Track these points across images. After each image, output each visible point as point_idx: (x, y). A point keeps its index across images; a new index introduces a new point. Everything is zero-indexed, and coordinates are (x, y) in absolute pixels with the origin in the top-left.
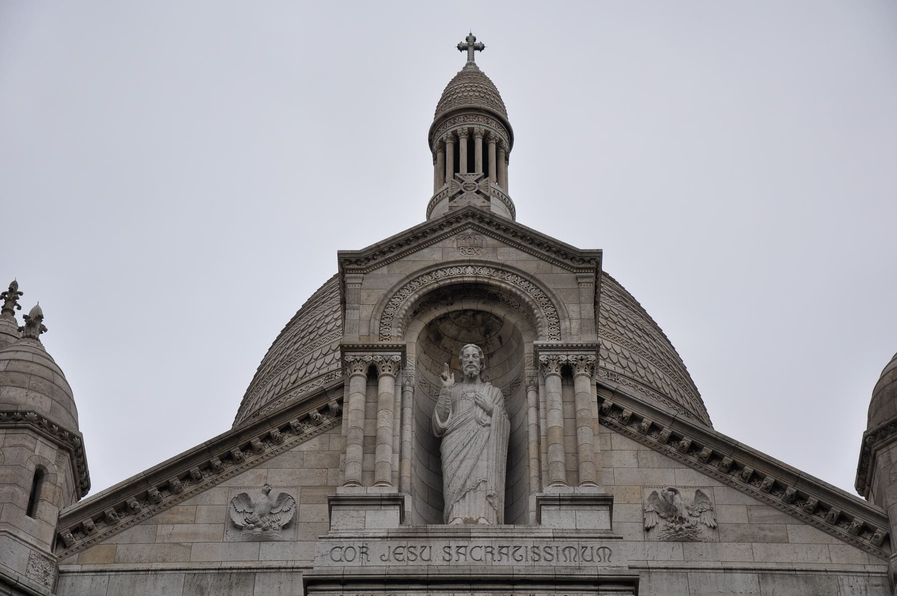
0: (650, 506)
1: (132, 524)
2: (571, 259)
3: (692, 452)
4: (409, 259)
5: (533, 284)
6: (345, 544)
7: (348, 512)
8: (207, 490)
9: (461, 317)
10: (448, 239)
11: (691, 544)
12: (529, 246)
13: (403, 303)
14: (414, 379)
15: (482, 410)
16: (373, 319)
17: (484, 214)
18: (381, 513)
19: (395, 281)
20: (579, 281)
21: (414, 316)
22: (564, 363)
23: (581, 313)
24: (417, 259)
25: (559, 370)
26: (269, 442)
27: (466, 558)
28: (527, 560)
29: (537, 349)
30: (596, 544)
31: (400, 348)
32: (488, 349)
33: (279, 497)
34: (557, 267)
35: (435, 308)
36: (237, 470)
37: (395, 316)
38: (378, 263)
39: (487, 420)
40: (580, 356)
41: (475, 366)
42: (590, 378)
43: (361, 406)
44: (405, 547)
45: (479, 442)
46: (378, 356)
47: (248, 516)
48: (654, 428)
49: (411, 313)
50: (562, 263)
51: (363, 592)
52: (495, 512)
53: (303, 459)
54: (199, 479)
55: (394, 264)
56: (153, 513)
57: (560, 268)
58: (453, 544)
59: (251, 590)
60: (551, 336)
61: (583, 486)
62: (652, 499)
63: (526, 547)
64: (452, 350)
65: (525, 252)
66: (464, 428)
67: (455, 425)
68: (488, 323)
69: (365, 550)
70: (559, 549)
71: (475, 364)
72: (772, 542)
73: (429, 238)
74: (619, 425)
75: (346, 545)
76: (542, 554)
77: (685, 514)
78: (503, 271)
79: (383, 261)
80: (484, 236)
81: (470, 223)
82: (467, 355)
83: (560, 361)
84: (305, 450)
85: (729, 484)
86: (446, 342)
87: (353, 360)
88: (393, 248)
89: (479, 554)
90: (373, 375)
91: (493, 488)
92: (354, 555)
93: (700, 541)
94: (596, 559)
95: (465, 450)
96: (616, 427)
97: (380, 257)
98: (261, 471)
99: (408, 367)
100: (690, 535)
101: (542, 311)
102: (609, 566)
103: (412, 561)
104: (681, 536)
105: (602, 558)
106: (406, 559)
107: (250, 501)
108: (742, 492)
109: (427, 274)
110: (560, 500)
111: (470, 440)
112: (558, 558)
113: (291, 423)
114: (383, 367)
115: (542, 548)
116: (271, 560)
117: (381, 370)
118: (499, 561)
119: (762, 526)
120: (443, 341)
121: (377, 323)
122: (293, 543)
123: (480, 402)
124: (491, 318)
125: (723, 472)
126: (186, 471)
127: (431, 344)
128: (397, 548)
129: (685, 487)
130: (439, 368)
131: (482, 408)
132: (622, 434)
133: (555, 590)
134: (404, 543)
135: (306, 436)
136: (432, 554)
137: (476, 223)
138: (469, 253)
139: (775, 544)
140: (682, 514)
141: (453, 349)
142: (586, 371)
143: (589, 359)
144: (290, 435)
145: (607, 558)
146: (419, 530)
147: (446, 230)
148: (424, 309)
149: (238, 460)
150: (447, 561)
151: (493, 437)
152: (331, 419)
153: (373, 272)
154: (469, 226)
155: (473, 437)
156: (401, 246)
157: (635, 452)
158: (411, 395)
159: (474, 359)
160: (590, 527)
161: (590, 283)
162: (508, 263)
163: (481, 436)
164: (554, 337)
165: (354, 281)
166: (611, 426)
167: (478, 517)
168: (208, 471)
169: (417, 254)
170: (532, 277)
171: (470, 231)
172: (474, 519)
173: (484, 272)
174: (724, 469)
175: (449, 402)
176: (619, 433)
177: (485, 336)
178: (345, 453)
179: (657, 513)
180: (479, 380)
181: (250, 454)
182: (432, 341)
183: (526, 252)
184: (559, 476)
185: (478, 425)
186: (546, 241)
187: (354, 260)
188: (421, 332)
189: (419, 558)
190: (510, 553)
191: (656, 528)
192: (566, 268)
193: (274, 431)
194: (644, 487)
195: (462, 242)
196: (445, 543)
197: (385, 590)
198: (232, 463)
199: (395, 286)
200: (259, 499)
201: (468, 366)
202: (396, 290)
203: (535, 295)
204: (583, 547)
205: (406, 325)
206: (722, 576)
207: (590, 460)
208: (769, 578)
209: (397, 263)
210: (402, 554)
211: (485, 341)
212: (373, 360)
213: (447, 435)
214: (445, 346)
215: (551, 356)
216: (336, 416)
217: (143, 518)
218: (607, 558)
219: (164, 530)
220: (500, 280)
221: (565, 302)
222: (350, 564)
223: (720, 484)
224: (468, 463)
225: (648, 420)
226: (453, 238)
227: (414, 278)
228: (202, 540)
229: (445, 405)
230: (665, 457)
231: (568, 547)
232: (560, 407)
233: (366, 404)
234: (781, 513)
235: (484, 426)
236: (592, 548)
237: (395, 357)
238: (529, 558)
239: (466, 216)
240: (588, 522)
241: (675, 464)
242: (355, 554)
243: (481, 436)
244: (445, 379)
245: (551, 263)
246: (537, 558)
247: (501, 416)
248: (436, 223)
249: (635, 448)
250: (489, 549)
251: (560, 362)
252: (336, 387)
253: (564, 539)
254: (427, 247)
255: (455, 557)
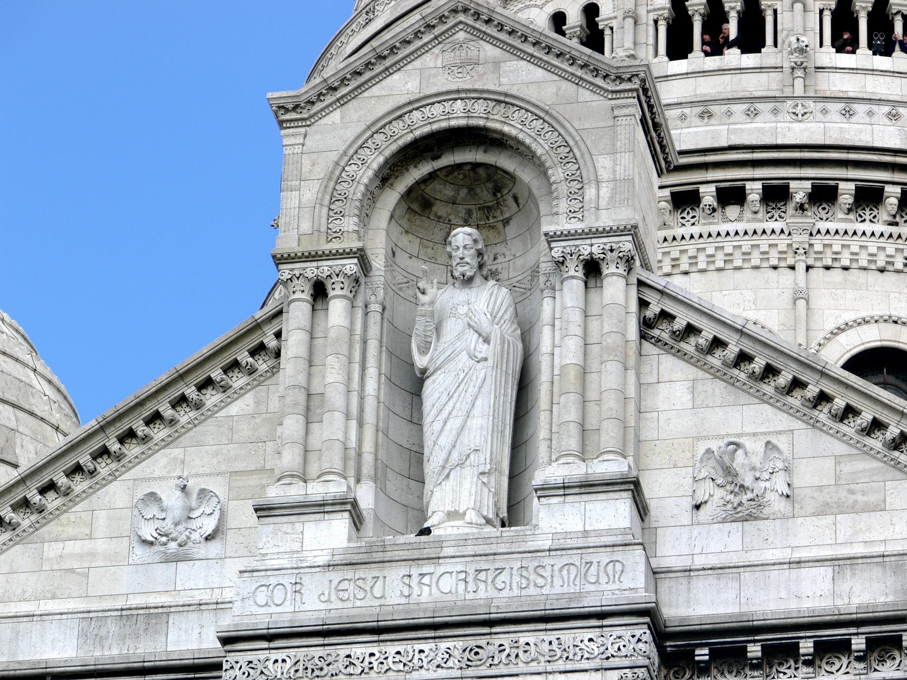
0: (703, 470)
1: (11, 543)
2: (605, 77)
3: (768, 378)
4: (371, 94)
5: (549, 124)
6: (273, 581)
7: (280, 525)
8: (105, 486)
9: (456, 173)
10: (430, 52)
11: (754, 523)
12: (545, 58)
13: (361, 172)
14: (382, 291)
15: (477, 335)
16: (317, 206)
17: (480, 9)
18: (324, 525)
19: (350, 133)
20: (616, 113)
21: (383, 185)
22: (586, 258)
23: (615, 171)
24: (384, 93)
25: (581, 267)
26: (184, 405)
27: (431, 590)
28: (511, 589)
29: (551, 238)
30: (604, 557)
31: (355, 253)
32: (502, 213)
33: (199, 494)
34: (584, 91)
35: (415, 167)
36: (143, 453)
37: (350, 197)
38: (327, 107)
39: (483, 349)
40: (609, 245)
41: (468, 263)
42: (625, 277)
43: (303, 351)
44: (352, 579)
45: (470, 389)
46: (324, 268)
47: (158, 524)
48: (717, 343)
49: (378, 183)
50: (591, 83)
51: (296, 650)
52: (491, 494)
53: (232, 429)
54: (93, 473)
55: (350, 105)
56: (37, 525)
57: (589, 92)
58: (415, 572)
59: (163, 638)
60: (572, 214)
61: (600, 461)
62: (705, 459)
63: (512, 568)
64: (450, 218)
65: (539, 66)
66: (451, 366)
67: (438, 362)
68: (495, 178)
69: (298, 587)
70: (555, 568)
71: (467, 260)
72: (863, 511)
73: (400, 56)
74: (671, 342)
75: (273, 581)
76: (533, 577)
77: (748, 481)
78: (506, 103)
79: (334, 102)
80: (482, 42)
81: (461, 22)
82: (455, 247)
83: (580, 255)
84: (234, 414)
85: (815, 424)
86: (440, 209)
87: (289, 277)
88: (348, 80)
89: (447, 584)
90: (319, 291)
91: (488, 461)
92: (283, 596)
93: (767, 519)
94: (603, 579)
95: (451, 403)
96: (666, 344)
97: (328, 97)
98: (175, 452)
99: (374, 272)
100: (754, 511)
101: (560, 170)
102: (619, 590)
103: (360, 599)
104: (741, 514)
105: (611, 577)
106: (352, 599)
107: (162, 503)
108: (832, 436)
109: (395, 119)
110: (564, 488)
111: (459, 386)
112: (552, 582)
113: (212, 376)
114: (333, 283)
115: (531, 569)
116: (192, 589)
117: (330, 289)
118: (475, 592)
119: (853, 487)
120: (434, 209)
121: (325, 210)
122: (219, 561)
123: (472, 323)
124: (498, 171)
125: (807, 407)
126: (74, 462)
127: (417, 216)
128: (340, 582)
129: (754, 434)
130: (433, 249)
131: (477, 332)
132: (674, 355)
133: (546, 630)
134: (349, 573)
135: (235, 392)
136: (387, 588)
137: (470, 21)
138: (460, 75)
139: (867, 514)
140: (744, 480)
141: (452, 217)
142: (617, 268)
143: (622, 250)
144: (214, 392)
145: (617, 576)
146: (375, 549)
147: (427, 38)
148: (397, 170)
149: (143, 439)
150: (406, 597)
151: (488, 380)
152: (269, 363)
153: (320, 121)
154: (461, 26)
155: (462, 381)
156: (360, 74)
157: (691, 383)
158: (378, 317)
159: (466, 252)
160: (603, 525)
161: (630, 115)
162: (514, 91)
163: (474, 378)
164: (574, 215)
165: (291, 141)
166: (660, 343)
167: (465, 509)
168: (105, 457)
169: (384, 83)
170: (547, 112)
171: (461, 36)
172: (461, 511)
173: (480, 107)
174: (807, 404)
175: (431, 325)
176: (670, 353)
177: (495, 195)
178: (281, 424)
179: (712, 479)
180: (478, 280)
181: (160, 426)
182: (416, 212)
183: (542, 68)
184: (570, 445)
185: (471, 361)
186: (568, 50)
187: (290, 106)
188: (394, 210)
189: (369, 595)
190: (490, 580)
191: (709, 503)
192: (598, 92)
193: (189, 391)
194: (699, 438)
195: (450, 57)
196: (403, 570)
197: (324, 645)
198: (136, 442)
199: (350, 146)
200: (172, 499)
201: (458, 264)
202: (351, 152)
203: (551, 143)
204: (587, 563)
205: (365, 216)
206: (787, 574)
207: (614, 416)
208: (848, 572)
209: (354, 101)
210: (347, 590)
211: (495, 202)
212: (317, 276)
213: (428, 377)
214: (439, 214)
215: (568, 248)
216: (276, 358)
217: (25, 534)
218: (617, 576)
219: (52, 550)
220: (503, 119)
221: (593, 151)
222: (279, 609)
223: (803, 426)
224: (454, 424)
225: (709, 331)
226: (436, 51)
227: (377, 127)
228: (101, 564)
229: (425, 331)
230: (730, 388)
231: (567, 564)
232: (579, 331)
233: (311, 342)
234: (881, 465)
235: (478, 362)
236: (599, 562)
237: (348, 267)
238: (514, 585)
239: (455, 11)
240: (601, 519)
241: (744, 398)
242: (286, 594)
243: (474, 378)
244: (423, 293)
245: (577, 84)
246: (524, 583)
247: (503, 340)
248: (410, 30)
249: (691, 377)
250: (462, 576)
251: (581, 257)
252: (272, 315)
253: (564, 552)
254: (399, 70)
255: (416, 590)
